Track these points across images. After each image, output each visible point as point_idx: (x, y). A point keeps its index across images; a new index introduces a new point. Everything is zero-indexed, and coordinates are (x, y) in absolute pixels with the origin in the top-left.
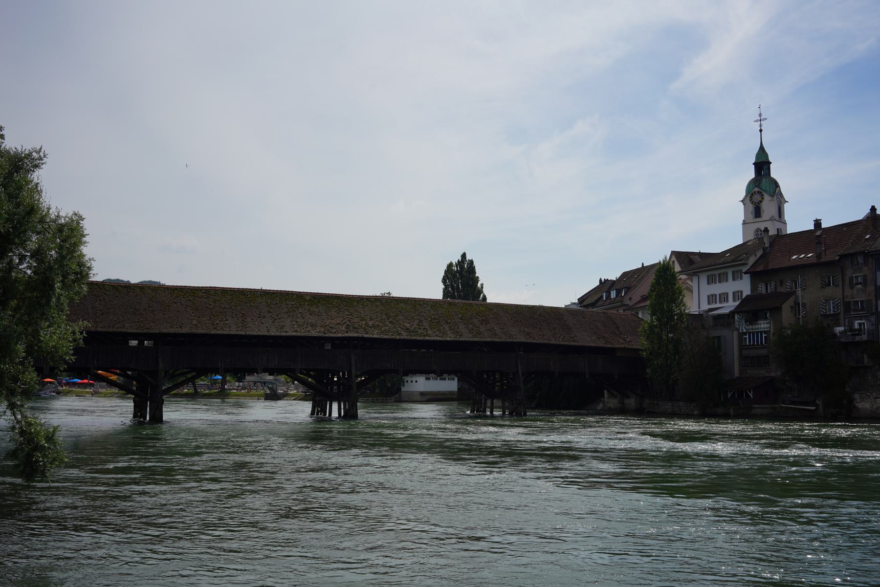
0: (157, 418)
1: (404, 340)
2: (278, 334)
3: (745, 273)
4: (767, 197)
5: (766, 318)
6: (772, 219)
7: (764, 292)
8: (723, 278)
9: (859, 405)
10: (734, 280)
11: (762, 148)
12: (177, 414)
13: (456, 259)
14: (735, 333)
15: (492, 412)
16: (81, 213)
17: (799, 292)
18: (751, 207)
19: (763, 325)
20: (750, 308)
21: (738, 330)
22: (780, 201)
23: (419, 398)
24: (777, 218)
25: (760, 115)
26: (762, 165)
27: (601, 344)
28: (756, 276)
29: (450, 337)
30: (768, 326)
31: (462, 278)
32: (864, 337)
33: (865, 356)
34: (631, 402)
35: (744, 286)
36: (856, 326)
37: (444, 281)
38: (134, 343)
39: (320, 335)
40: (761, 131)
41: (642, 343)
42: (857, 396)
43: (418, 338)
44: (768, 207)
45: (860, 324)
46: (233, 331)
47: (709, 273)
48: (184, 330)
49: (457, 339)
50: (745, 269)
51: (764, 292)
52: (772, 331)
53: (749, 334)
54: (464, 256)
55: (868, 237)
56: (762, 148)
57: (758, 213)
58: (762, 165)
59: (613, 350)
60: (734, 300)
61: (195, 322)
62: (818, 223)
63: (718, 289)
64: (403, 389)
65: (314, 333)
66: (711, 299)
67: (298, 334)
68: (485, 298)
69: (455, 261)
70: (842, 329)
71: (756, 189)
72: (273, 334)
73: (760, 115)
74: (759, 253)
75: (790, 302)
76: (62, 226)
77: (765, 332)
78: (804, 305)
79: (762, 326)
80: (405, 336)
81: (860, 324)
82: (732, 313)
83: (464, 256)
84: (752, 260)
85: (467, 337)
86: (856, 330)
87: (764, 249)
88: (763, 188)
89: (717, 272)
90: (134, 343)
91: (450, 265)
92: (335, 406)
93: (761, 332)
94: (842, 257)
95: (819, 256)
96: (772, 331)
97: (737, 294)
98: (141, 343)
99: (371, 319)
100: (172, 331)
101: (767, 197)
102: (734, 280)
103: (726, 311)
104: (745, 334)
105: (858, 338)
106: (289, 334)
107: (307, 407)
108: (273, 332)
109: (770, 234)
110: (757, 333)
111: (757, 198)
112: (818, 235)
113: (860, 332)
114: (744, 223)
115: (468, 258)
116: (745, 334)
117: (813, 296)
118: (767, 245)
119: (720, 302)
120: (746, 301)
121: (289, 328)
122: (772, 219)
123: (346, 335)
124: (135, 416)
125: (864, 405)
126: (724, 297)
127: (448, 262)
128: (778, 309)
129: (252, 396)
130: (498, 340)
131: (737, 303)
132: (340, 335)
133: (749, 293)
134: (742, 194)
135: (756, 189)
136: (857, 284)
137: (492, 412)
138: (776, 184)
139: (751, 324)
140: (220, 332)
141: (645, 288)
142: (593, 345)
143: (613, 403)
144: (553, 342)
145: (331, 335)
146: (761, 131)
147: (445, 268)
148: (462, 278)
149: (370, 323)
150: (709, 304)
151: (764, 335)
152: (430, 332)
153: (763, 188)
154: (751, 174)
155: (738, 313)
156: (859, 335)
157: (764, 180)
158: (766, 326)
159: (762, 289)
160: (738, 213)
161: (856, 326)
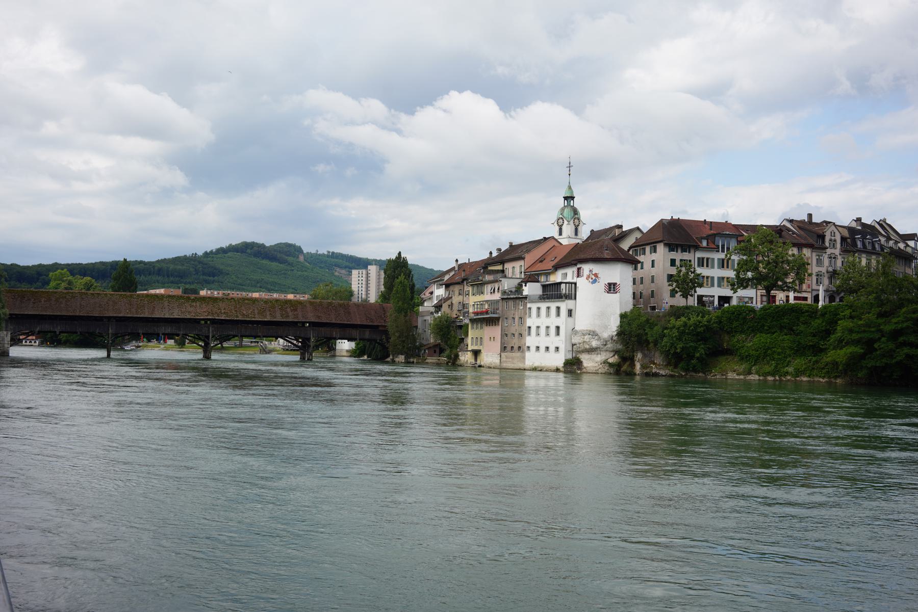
13: (394, 257)
18: (557, 228)
23: (345, 354)
24: (573, 236)
26: (569, 198)
28: (447, 286)
29: (268, 319)
46: (146, 315)
54: (400, 253)
56: (570, 188)
58: (569, 198)
59: (378, 326)
65: (188, 317)
74: (452, 273)
75: (449, 302)
80: (240, 318)
83: (400, 253)
84: (447, 278)
85: (279, 318)
101: (566, 222)
108: (167, 316)
109: (459, 263)
115: (402, 256)
144: (334, 321)
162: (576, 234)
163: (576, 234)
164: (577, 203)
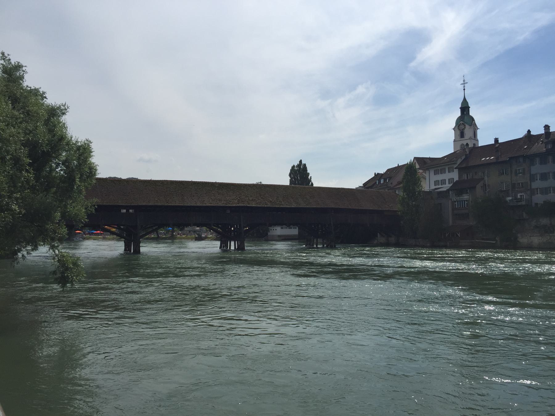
0: (137, 251)
1: (269, 207)
2: (201, 205)
3: (455, 168)
4: (467, 126)
5: (467, 193)
6: (470, 139)
7: (466, 178)
8: (443, 172)
9: (521, 240)
10: (449, 172)
11: (465, 99)
12: (148, 249)
13: (296, 163)
14: (450, 201)
15: (317, 246)
16: (90, 139)
17: (486, 178)
19: (466, 197)
20: (458, 188)
21: (451, 200)
22: (475, 128)
24: (473, 138)
26: (465, 108)
27: (376, 208)
29: (294, 205)
31: (300, 173)
32: (523, 203)
33: (524, 213)
34: (393, 239)
35: (455, 176)
36: (519, 197)
37: (290, 175)
38: (124, 211)
39: (224, 205)
40: (464, 89)
41: (398, 207)
42: (519, 235)
43: (277, 206)
44: (468, 132)
45: (521, 196)
48: (150, 204)
49: (298, 206)
50: (455, 166)
51: (466, 178)
53: (458, 202)
54: (301, 161)
55: (526, 147)
56: (465, 99)
57: (462, 135)
58: (465, 108)
60: (449, 183)
61: (156, 199)
62: (496, 140)
63: (440, 177)
64: (269, 234)
65: (220, 204)
66: (436, 183)
67: (212, 205)
68: (312, 184)
69: (296, 164)
70: (510, 198)
71: (462, 122)
72: (198, 205)
73: (464, 81)
74: (463, 157)
75: (481, 184)
76: (80, 147)
77: (467, 201)
78: (489, 186)
80: (269, 205)
81: (521, 196)
82: (448, 191)
83: (301, 161)
84: (459, 161)
85: (303, 205)
86: (519, 199)
87: (466, 155)
88: (465, 122)
89: (439, 168)
90: (124, 211)
91: (293, 167)
92: (232, 243)
93: (464, 201)
94: (511, 158)
95: (497, 158)
97: (451, 180)
98: (128, 211)
99: (251, 196)
100: (144, 204)
101: (467, 126)
102: (449, 172)
103: (445, 189)
104: (455, 202)
105: (520, 204)
106: (207, 205)
107: (218, 243)
108: (199, 204)
110: (462, 201)
112: (497, 147)
113: (521, 200)
114: (455, 141)
115: (303, 162)
116: (455, 202)
117: (494, 180)
118: (468, 153)
119: (441, 185)
120: (456, 184)
121: (208, 202)
122: (470, 139)
123: (238, 205)
124: (125, 250)
125: (523, 240)
126: (443, 182)
127: (411, 19)
128: (474, 188)
129: (188, 239)
130: (319, 207)
131: (451, 185)
132: (234, 205)
134: (453, 125)
136: (520, 173)
137: (317, 246)
138: (473, 119)
139: (458, 196)
140: (170, 204)
141: (400, 176)
142: (371, 209)
143: (383, 240)
144: (350, 207)
145: (230, 205)
146: (464, 89)
147: (291, 168)
148: (300, 173)
149: (251, 199)
150: (435, 185)
152: (283, 203)
153: (465, 122)
154: (458, 114)
155: (451, 190)
156: (519, 201)
157: (466, 117)
159: (465, 177)
160: (451, 135)
161: (519, 197)
162: (475, 137)
163: (475, 137)
164: (472, 113)
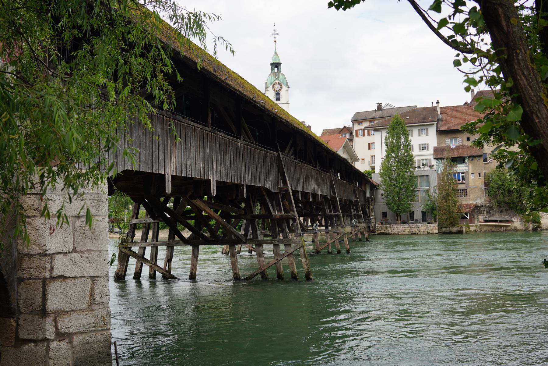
10: (419, 135)
25: (275, 31)
26: (276, 65)
30: (467, 168)
40: (275, 42)
47: (420, 128)
52: (470, 172)
56: (276, 53)
58: (276, 65)
73: (275, 31)
77: (463, 173)
79: (461, 168)
93: (459, 173)
96: (470, 172)
111: (277, 87)
133: (436, 145)
135: (277, 81)
146: (275, 42)
151: (461, 175)
158: (464, 168)
